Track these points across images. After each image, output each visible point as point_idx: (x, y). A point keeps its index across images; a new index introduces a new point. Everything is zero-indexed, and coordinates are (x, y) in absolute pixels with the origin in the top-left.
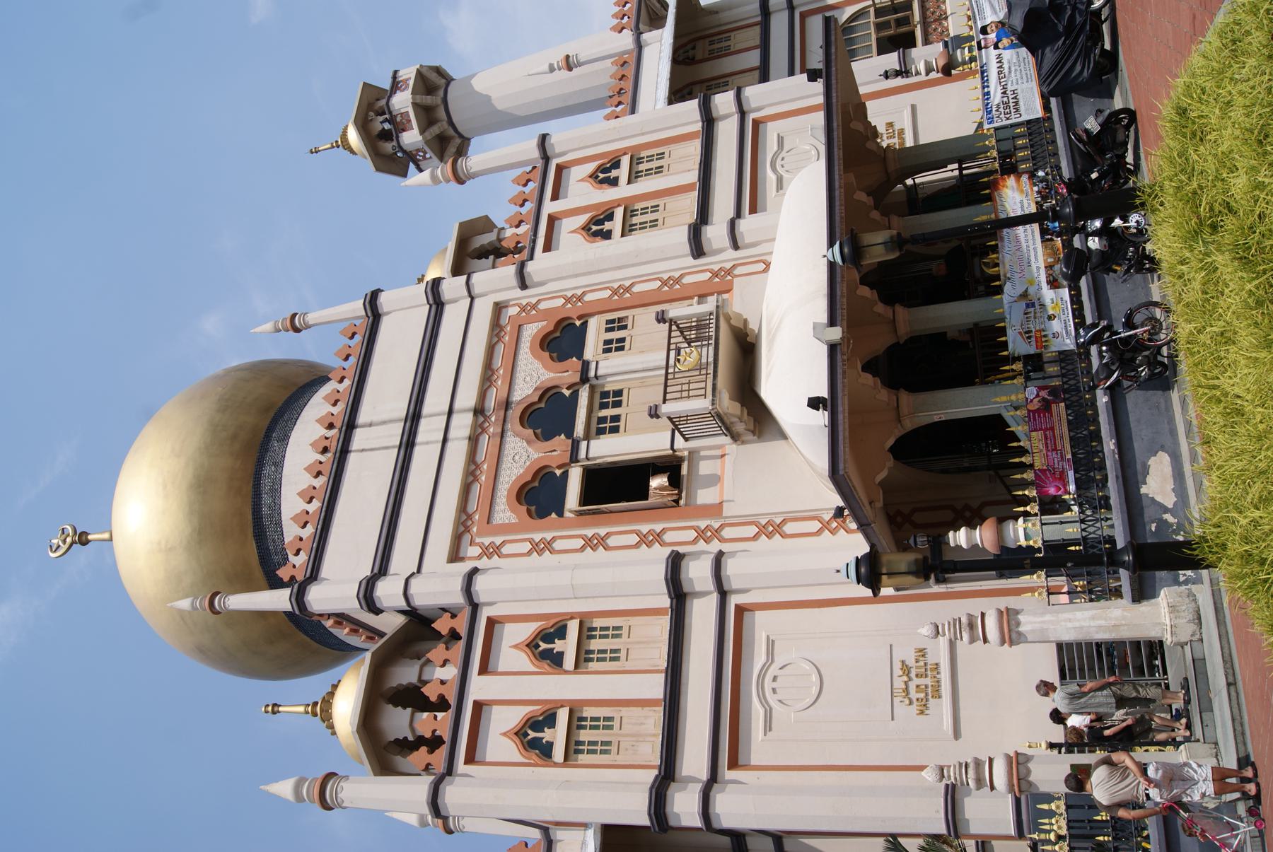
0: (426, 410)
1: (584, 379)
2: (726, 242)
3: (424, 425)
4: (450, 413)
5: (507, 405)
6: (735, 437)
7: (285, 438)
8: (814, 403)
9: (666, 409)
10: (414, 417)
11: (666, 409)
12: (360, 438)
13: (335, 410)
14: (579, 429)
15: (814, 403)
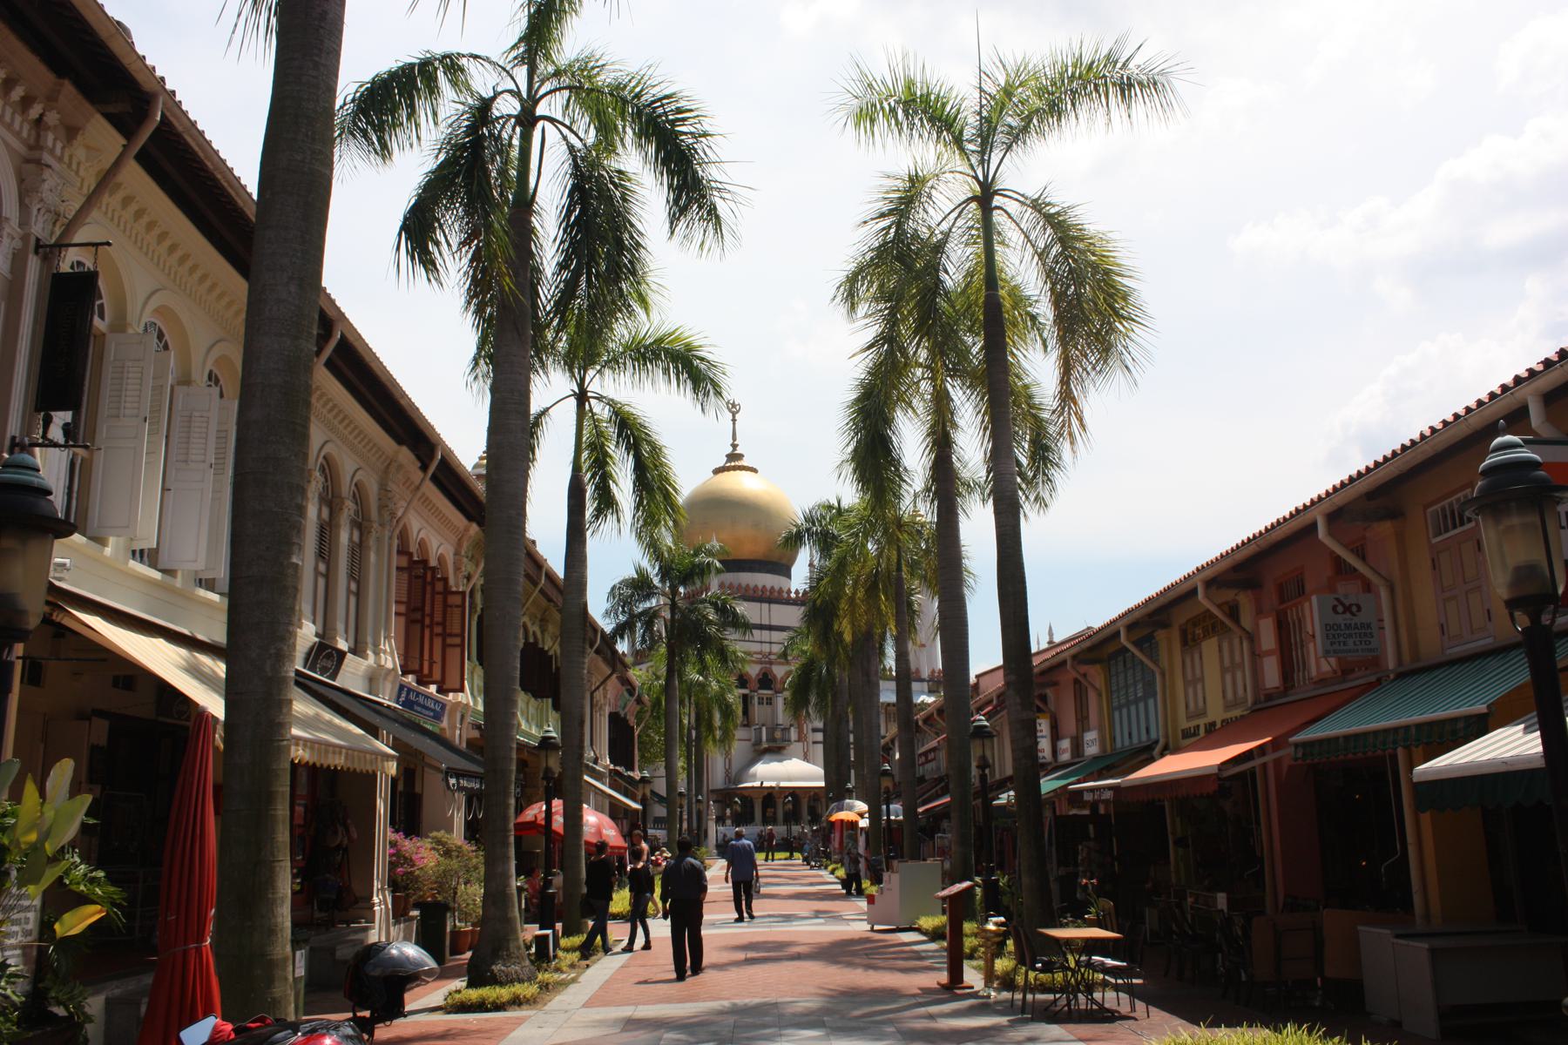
0: (773, 633)
1: (777, 692)
2: (815, 740)
3: (767, 632)
4: (771, 643)
5: (771, 663)
6: (754, 745)
7: (768, 572)
8: (762, 783)
9: (764, 729)
10: (770, 628)
11: (764, 729)
12: (765, 606)
13: (776, 594)
14: (761, 691)
15: (762, 783)
